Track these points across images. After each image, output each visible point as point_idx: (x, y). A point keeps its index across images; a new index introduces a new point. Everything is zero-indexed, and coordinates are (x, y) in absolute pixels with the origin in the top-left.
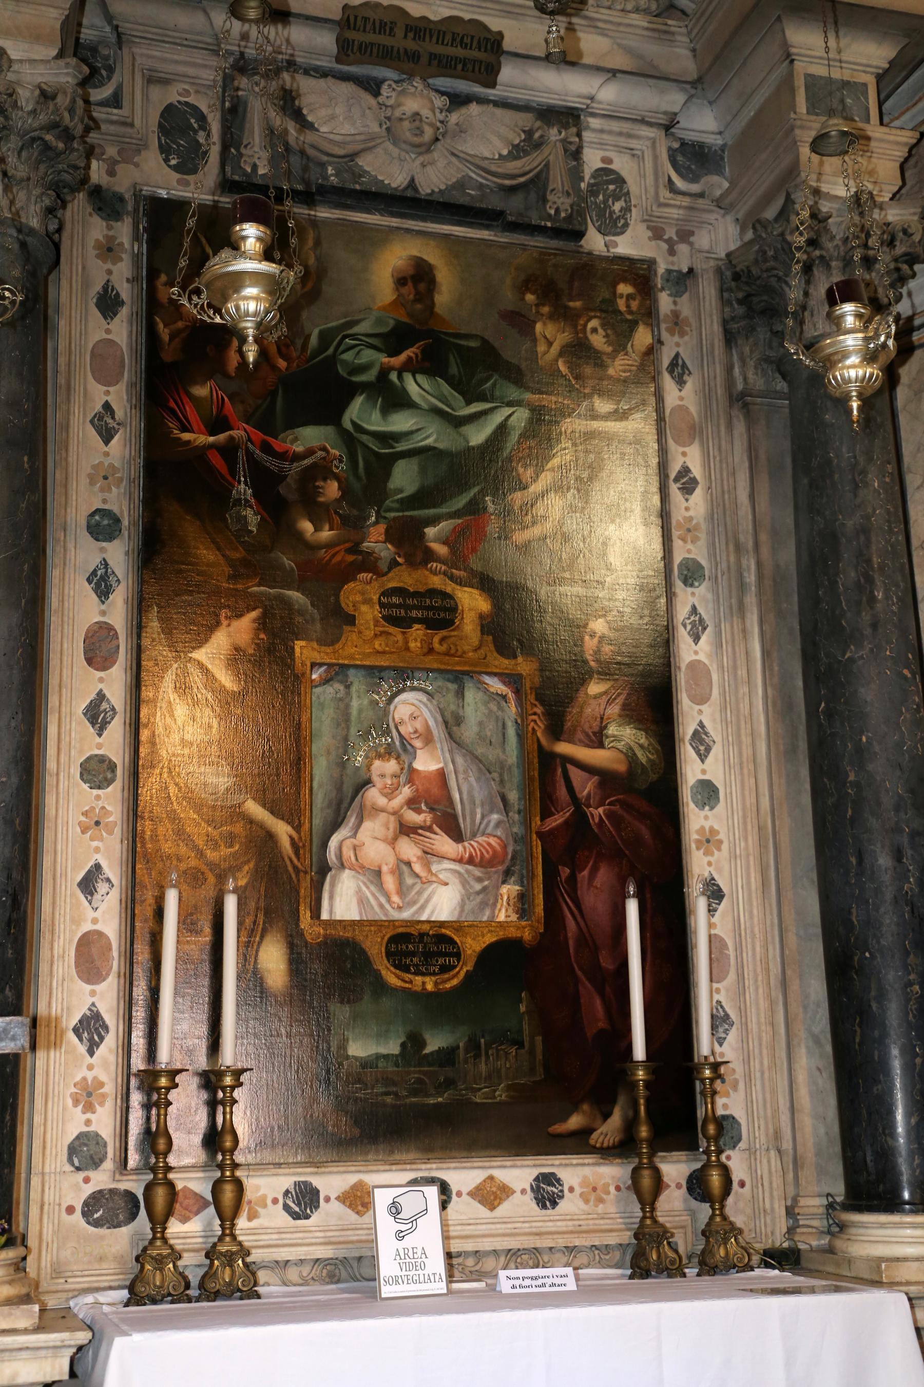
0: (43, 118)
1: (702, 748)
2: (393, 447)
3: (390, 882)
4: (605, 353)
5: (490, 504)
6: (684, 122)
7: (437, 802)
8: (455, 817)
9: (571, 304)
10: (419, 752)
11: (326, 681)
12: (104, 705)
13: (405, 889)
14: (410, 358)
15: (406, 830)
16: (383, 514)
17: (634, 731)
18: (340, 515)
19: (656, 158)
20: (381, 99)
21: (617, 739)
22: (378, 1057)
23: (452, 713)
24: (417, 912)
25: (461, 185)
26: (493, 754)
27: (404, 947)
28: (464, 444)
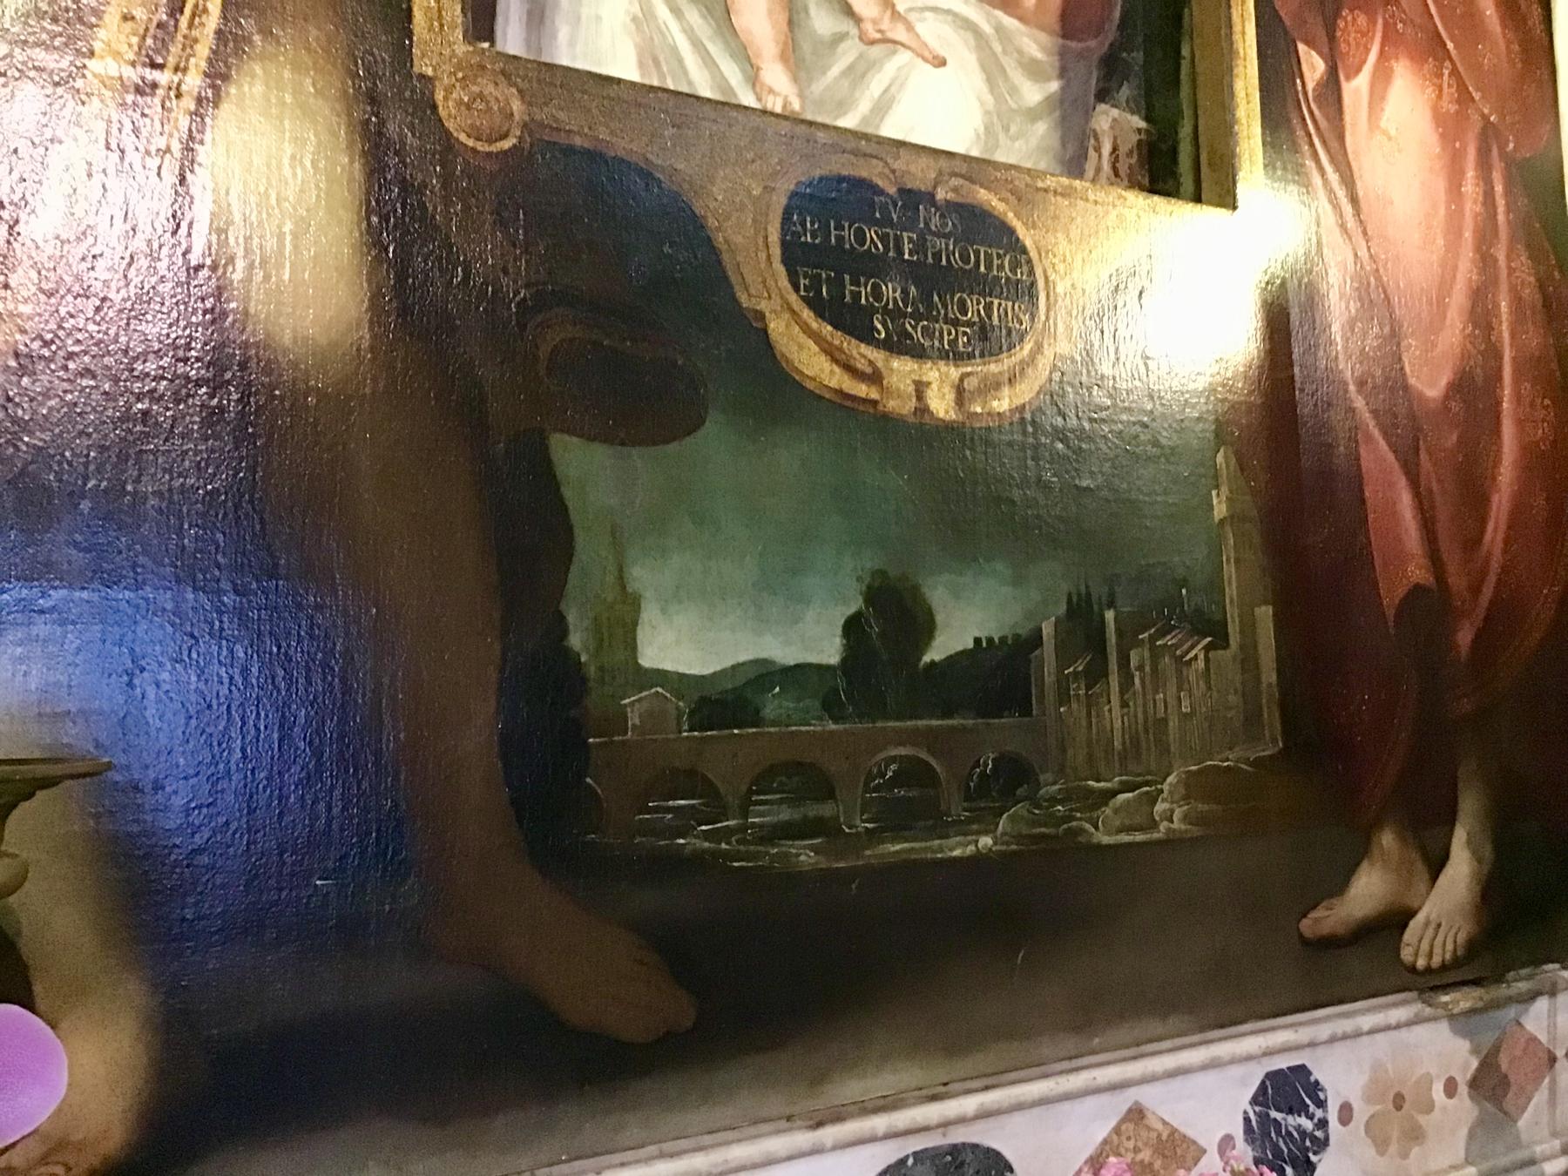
13: (806, 47)
22: (765, 675)
27: (849, 234)
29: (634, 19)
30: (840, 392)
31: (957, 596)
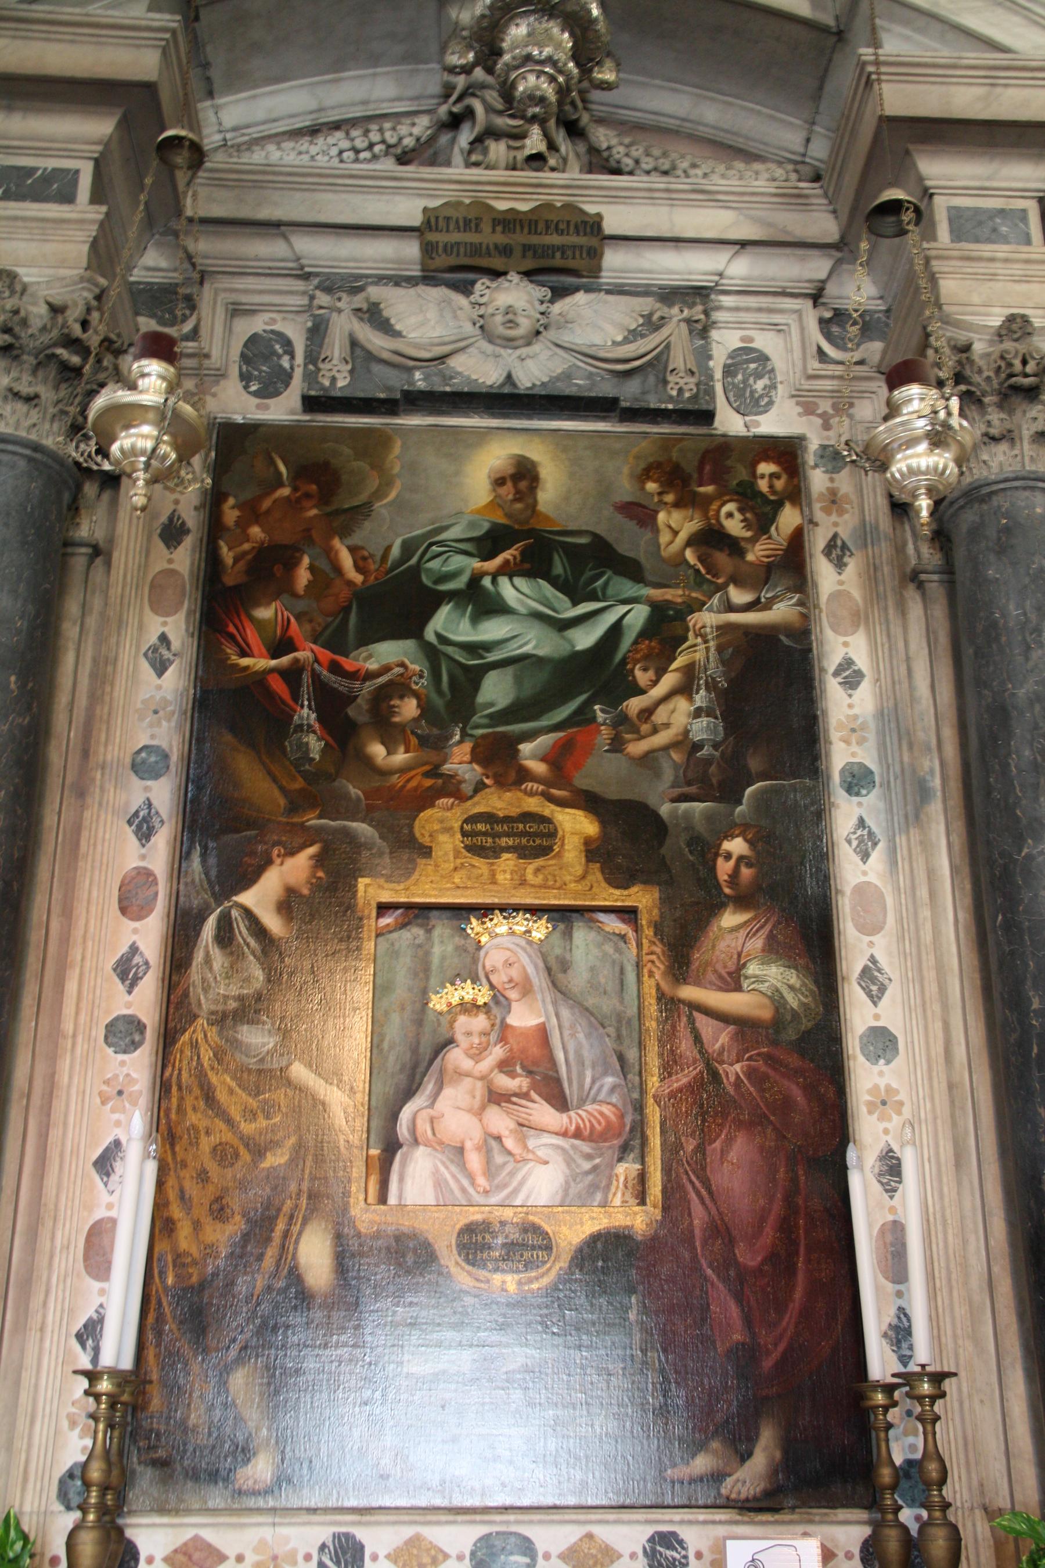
0: (55, 333)
1: (874, 988)
2: (482, 658)
3: (474, 1160)
4: (744, 539)
5: (599, 713)
6: (831, 289)
7: (535, 1063)
8: (558, 1081)
9: (702, 489)
10: (514, 1004)
11: (403, 926)
12: (137, 959)
13: (493, 1169)
14: (507, 562)
15: (496, 1098)
16: (470, 732)
17: (782, 969)
18: (418, 736)
19: (802, 329)
20: (472, 298)
21: (759, 980)
23: (557, 957)
24: (508, 1197)
25: (567, 376)
26: (607, 1005)
27: (480, 1238)
28: (568, 648)
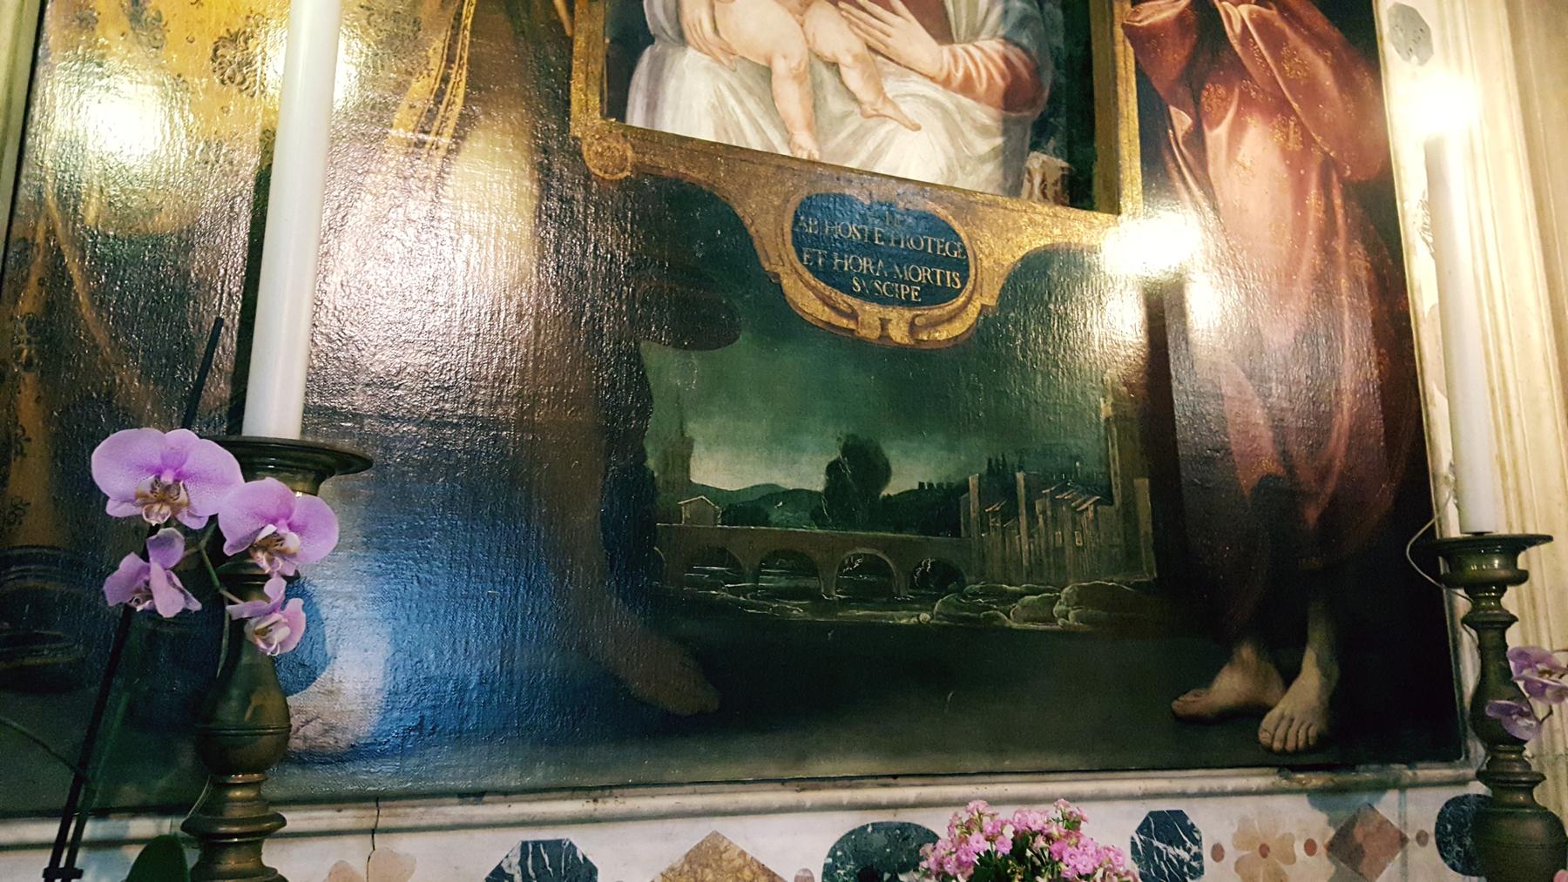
3: (791, 98)
22: (773, 495)
29: (713, 106)
30: (828, 323)
31: (906, 453)
